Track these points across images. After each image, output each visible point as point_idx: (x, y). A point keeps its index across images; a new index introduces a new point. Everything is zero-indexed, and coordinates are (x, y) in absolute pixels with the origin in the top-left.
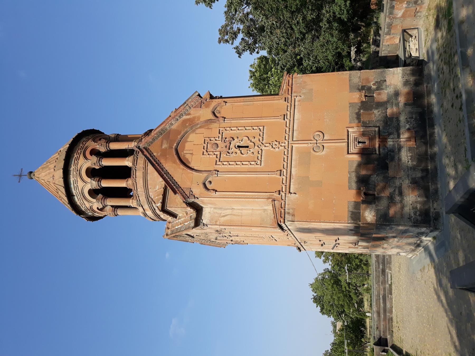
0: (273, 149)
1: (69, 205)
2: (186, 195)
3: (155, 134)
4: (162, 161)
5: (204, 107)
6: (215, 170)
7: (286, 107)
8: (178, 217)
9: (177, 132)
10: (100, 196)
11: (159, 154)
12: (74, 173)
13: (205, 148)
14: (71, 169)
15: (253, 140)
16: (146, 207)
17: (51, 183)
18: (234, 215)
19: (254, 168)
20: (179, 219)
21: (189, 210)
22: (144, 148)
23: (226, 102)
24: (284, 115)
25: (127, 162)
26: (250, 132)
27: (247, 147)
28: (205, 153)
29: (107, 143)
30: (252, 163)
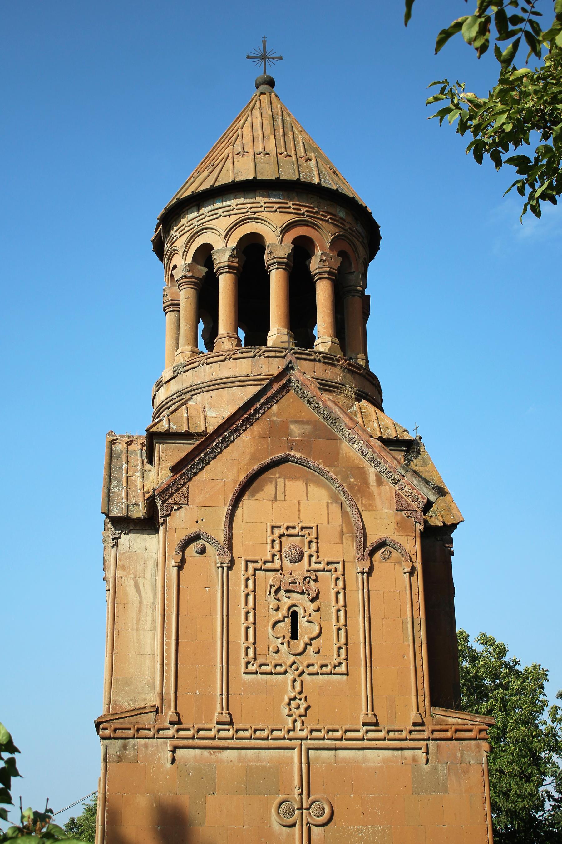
0: (287, 700)
2: (172, 494)
3: (324, 403)
4: (257, 428)
5: (399, 518)
7: (397, 728)
8: (148, 466)
9: (332, 458)
10: (202, 270)
11: (275, 418)
12: (249, 206)
13: (291, 531)
14: (258, 199)
15: (310, 649)
16: (174, 387)
17: (231, 147)
18: (140, 611)
19: (238, 658)
22: (290, 381)
24: (377, 724)
25: (277, 332)
26: (330, 642)
27: (294, 635)
28: (277, 532)
29: (329, 273)
30: (251, 652)
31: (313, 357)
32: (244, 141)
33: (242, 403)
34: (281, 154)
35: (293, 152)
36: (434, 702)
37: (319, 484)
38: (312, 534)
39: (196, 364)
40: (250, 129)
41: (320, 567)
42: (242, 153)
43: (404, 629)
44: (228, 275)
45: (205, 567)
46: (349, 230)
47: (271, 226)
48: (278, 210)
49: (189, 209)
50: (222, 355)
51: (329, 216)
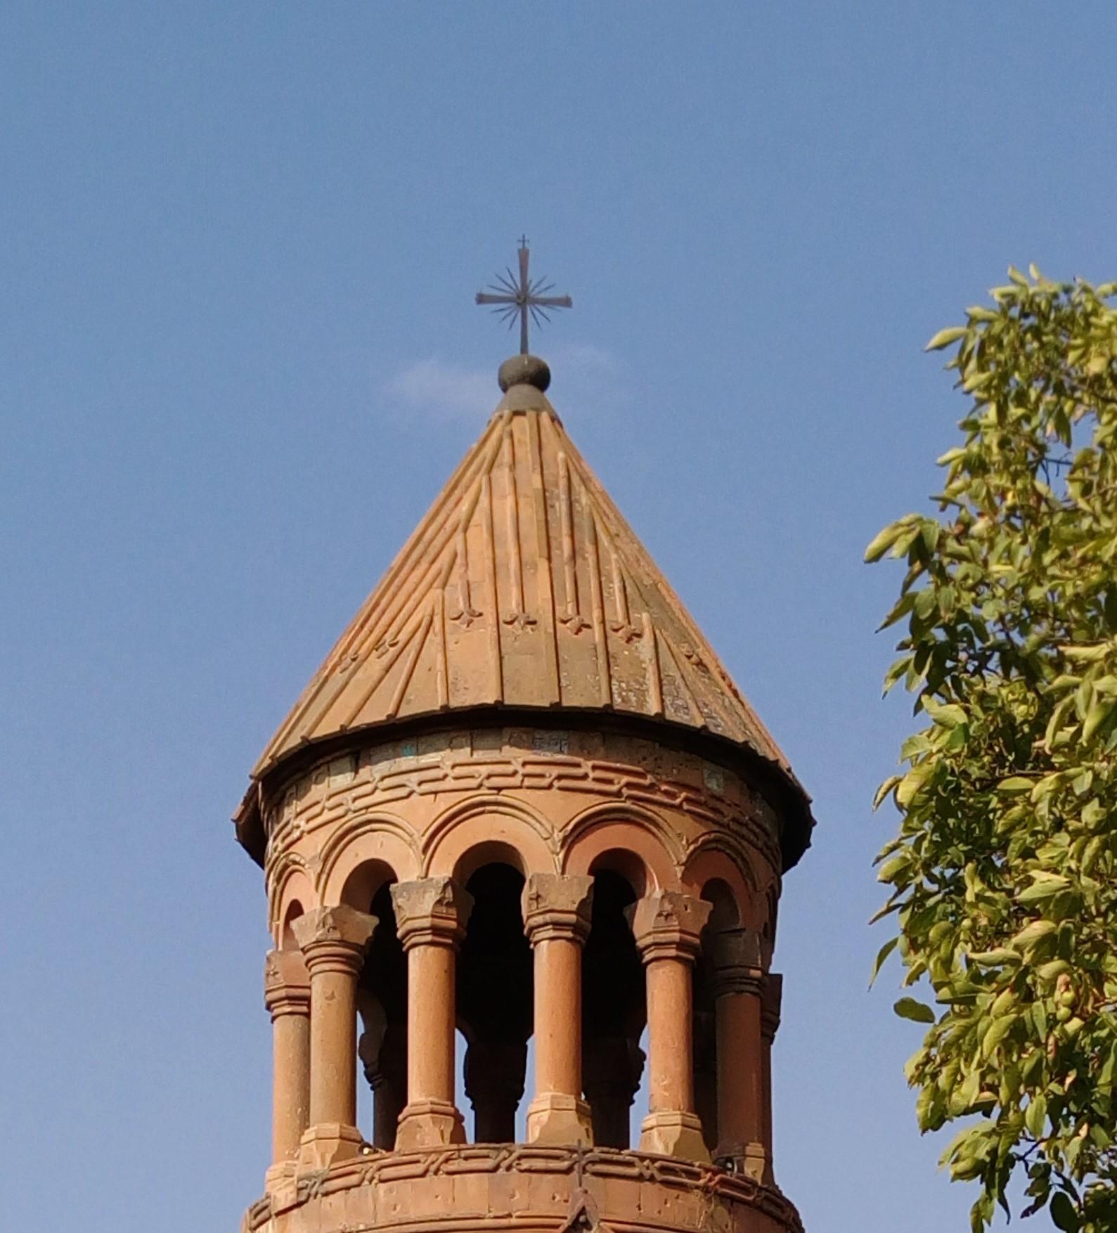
1: (294, 741)
10: (366, 924)
12: (485, 770)
14: (508, 752)
17: (436, 593)
31: (634, 1171)
32: (471, 576)
34: (565, 622)
35: (596, 613)
39: (354, 1179)
40: (485, 536)
42: (466, 616)
44: (431, 949)
46: (734, 826)
47: (538, 826)
48: (556, 784)
49: (333, 760)
50: (418, 1162)
51: (683, 795)
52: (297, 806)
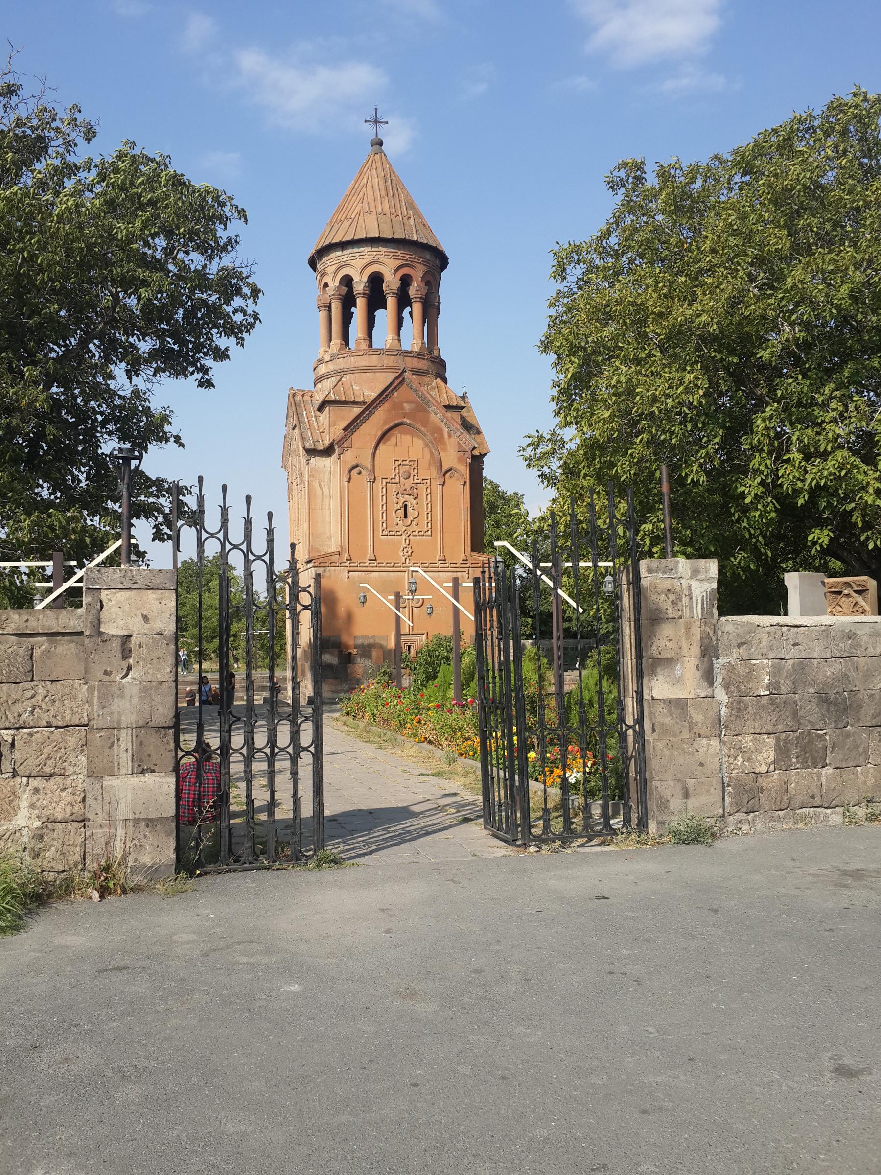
1: (327, 243)
4: (386, 406)
6: (375, 479)
8: (318, 413)
9: (426, 422)
13: (404, 463)
14: (381, 248)
15: (414, 523)
16: (331, 367)
20: (316, 416)
21: (327, 442)
23: (464, 485)
26: (423, 520)
27: (406, 517)
29: (421, 298)
30: (385, 525)
33: (380, 390)
36: (473, 549)
37: (419, 437)
38: (415, 464)
41: (419, 481)
43: (460, 513)
45: (362, 481)
52: (328, 258)
